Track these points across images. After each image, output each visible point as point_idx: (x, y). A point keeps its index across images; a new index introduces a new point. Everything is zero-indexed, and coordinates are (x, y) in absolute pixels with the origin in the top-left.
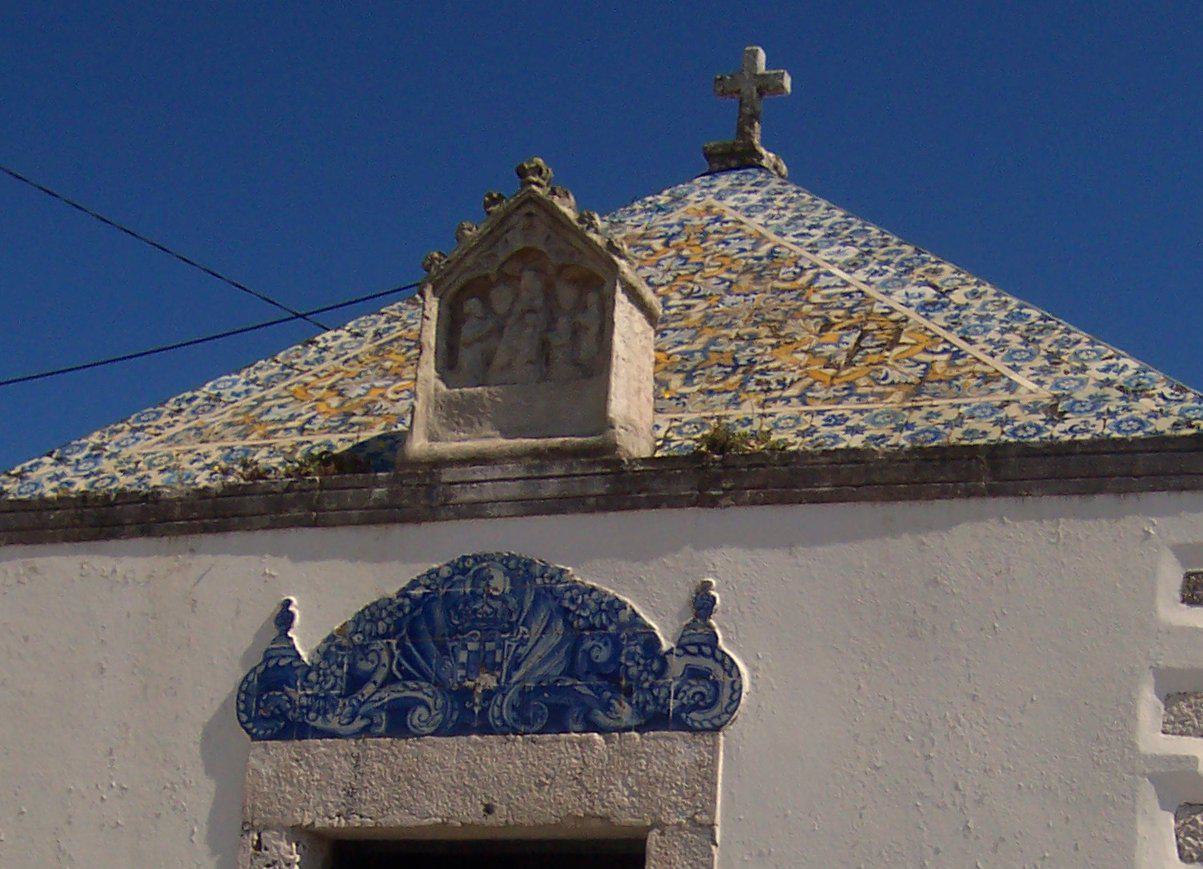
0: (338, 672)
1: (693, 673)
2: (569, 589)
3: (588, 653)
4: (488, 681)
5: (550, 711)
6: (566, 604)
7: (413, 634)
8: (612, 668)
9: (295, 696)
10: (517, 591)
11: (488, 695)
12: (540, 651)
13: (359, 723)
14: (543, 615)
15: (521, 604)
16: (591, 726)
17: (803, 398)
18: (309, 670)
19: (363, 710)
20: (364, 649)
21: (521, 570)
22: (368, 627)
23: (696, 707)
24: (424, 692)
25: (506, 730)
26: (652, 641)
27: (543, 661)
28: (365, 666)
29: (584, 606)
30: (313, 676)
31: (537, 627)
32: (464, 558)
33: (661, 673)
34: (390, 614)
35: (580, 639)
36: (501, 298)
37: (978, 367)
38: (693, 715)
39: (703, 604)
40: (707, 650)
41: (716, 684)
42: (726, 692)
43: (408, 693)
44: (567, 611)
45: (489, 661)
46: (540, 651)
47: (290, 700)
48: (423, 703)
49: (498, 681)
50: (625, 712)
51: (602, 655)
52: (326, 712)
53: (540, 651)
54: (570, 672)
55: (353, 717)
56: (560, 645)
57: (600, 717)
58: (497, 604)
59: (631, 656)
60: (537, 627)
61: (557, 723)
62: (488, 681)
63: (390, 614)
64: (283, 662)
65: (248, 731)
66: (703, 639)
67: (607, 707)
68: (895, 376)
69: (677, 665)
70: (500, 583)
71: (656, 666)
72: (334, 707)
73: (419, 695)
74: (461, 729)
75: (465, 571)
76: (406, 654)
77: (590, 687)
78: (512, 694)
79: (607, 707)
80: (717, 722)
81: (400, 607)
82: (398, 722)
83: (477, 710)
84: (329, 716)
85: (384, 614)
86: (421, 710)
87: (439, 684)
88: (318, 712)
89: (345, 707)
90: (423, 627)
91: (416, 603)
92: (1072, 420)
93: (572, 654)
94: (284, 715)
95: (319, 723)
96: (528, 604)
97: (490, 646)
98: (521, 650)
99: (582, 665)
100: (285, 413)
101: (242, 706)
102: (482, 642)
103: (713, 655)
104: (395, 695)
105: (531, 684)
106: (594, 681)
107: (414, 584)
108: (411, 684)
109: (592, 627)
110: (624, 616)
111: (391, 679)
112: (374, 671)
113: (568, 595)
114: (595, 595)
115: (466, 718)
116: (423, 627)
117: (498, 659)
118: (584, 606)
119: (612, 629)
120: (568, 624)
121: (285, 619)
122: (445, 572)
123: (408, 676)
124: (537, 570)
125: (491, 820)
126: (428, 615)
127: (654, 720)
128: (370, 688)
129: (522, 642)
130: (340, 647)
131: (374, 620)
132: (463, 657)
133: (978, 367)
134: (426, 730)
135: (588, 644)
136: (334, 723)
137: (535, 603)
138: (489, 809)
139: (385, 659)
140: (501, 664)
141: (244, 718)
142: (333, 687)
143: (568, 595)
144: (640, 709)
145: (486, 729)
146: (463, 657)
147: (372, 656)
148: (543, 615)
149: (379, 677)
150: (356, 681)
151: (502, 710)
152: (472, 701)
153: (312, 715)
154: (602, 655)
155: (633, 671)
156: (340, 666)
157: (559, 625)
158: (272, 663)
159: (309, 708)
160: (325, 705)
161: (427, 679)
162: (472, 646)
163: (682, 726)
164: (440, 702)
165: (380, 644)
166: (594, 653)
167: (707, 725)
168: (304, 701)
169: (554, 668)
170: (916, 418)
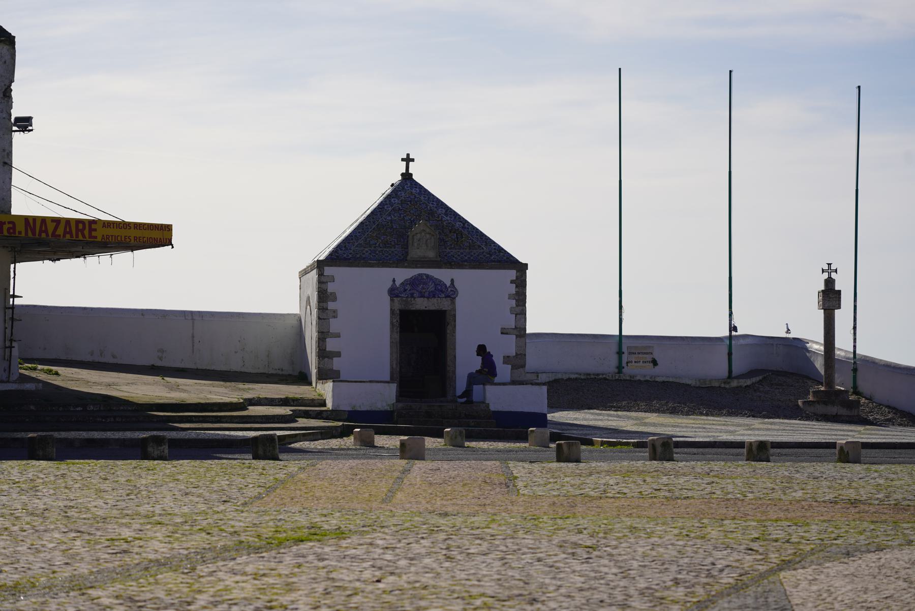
5: (433, 295)
12: (431, 287)
21: (427, 276)
39: (452, 280)
61: (434, 297)
82: (412, 296)
121: (394, 281)
127: (447, 296)
145: (424, 297)
150: (405, 290)
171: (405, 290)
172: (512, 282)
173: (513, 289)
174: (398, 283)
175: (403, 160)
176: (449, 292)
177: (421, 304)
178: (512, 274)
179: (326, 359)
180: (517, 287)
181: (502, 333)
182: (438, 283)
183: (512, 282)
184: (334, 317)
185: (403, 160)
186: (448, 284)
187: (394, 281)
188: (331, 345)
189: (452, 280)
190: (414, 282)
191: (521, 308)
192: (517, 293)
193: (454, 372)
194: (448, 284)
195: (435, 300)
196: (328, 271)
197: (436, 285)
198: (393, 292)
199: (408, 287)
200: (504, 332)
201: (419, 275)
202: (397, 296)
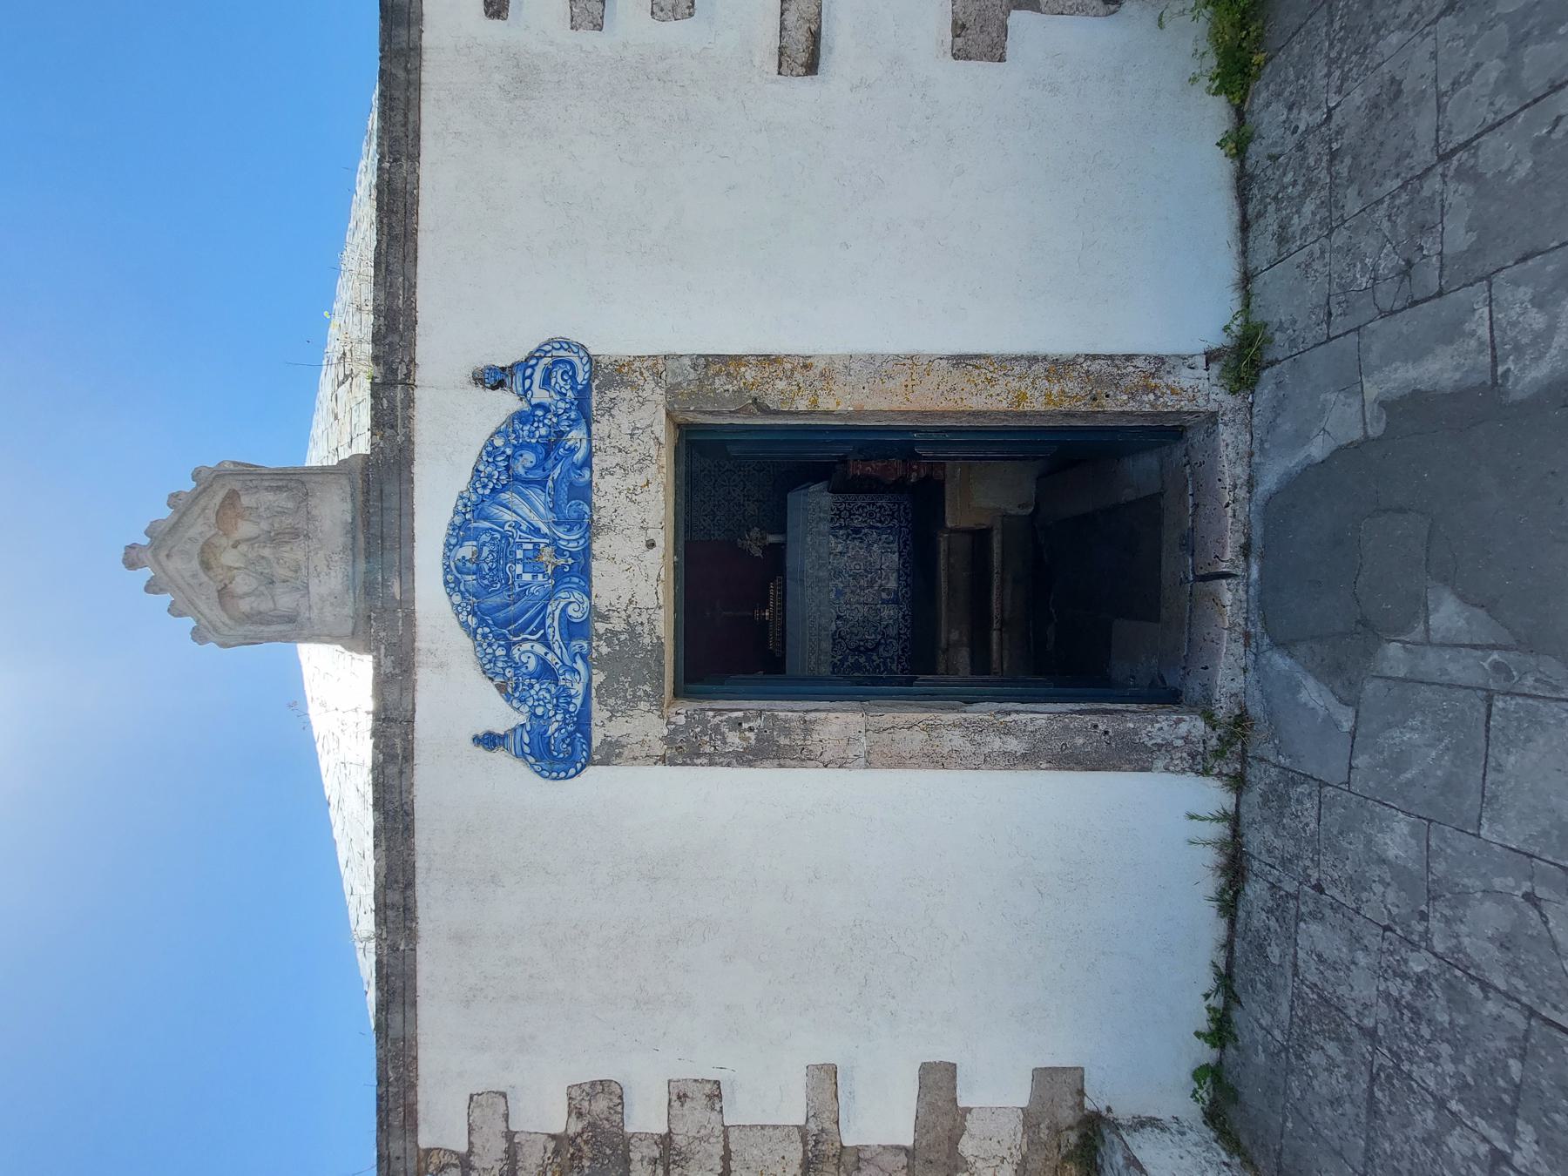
0: (537, 687)
2: (475, 490)
3: (528, 470)
6: (487, 492)
8: (540, 449)
9: (556, 725)
11: (559, 552)
13: (580, 665)
15: (486, 530)
16: (587, 463)
19: (568, 662)
21: (460, 532)
22: (500, 664)
24: (554, 608)
26: (521, 417)
28: (532, 664)
30: (539, 711)
31: (507, 516)
32: (446, 583)
34: (490, 645)
35: (517, 478)
38: (579, 379)
39: (494, 379)
40: (529, 372)
41: (555, 364)
42: (562, 353)
43: (556, 624)
44: (493, 490)
45: (530, 554)
47: (558, 730)
48: (564, 610)
49: (548, 545)
50: (576, 436)
51: (529, 458)
52: (570, 696)
54: (542, 484)
55: (575, 671)
56: (520, 494)
57: (579, 456)
58: (486, 550)
60: (507, 516)
61: (583, 493)
62: (547, 554)
63: (490, 645)
64: (526, 740)
65: (584, 767)
66: (519, 376)
67: (572, 451)
69: (539, 395)
70: (467, 550)
71: (540, 413)
72: (565, 689)
73: (557, 613)
74: (585, 573)
75: (457, 581)
76: (523, 629)
77: (554, 467)
78: (560, 532)
80: (585, 360)
81: (485, 636)
83: (571, 561)
84: (573, 692)
85: (489, 651)
88: (569, 703)
89: (565, 679)
93: (528, 483)
94: (570, 734)
95: (578, 701)
96: (487, 524)
97: (520, 554)
98: (524, 528)
99: (538, 474)
101: (563, 774)
102: (516, 561)
103: (532, 367)
104: (557, 636)
105: (551, 516)
106: (549, 464)
107: (464, 625)
108: (548, 622)
109: (508, 468)
111: (544, 641)
112: (537, 656)
113: (480, 491)
114: (481, 468)
115: (578, 570)
116: (501, 615)
117: (530, 546)
118: (490, 477)
119: (509, 451)
121: (489, 741)
122: (457, 599)
123: (542, 624)
125: (660, 542)
128: (550, 657)
130: (515, 689)
132: (527, 577)
134: (587, 603)
135: (521, 471)
136: (578, 688)
137: (486, 519)
139: (526, 646)
140: (535, 544)
141: (572, 771)
142: (549, 691)
143: (480, 491)
144: (573, 423)
145: (587, 551)
146: (527, 577)
147: (524, 659)
148: (495, 511)
149: (540, 649)
151: (570, 540)
152: (563, 566)
153: (572, 708)
155: (543, 431)
156: (531, 686)
157: (505, 496)
158: (527, 749)
159: (567, 711)
161: (545, 606)
162: (519, 568)
164: (563, 595)
165: (515, 652)
166: (529, 465)
167: (587, 368)
168: (559, 717)
169: (539, 498)
171: (546, 671)
179: (967, 1147)
184: (715, 1095)
187: (489, 741)
189: (494, 379)
194: (507, 403)
195: (608, 491)
197: (517, 481)
198: (559, 749)
199: (528, 652)
201: (452, 584)
202: (582, 722)
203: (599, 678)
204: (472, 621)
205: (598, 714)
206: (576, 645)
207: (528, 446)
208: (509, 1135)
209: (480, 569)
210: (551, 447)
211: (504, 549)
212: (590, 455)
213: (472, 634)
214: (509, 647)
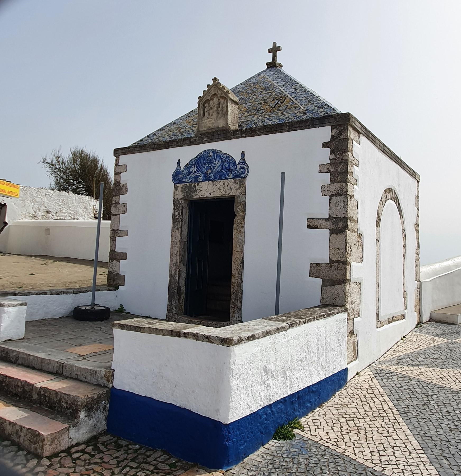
1: (241, 168)
4: (210, 171)
5: (219, 176)
7: (198, 164)
10: (214, 155)
11: (210, 174)
12: (218, 165)
13: (190, 180)
14: (218, 159)
16: (226, 178)
17: (264, 115)
18: (183, 171)
20: (191, 167)
21: (214, 151)
23: (242, 174)
24: (200, 174)
25: (213, 180)
26: (235, 162)
27: (218, 167)
28: (191, 170)
29: (224, 157)
31: (217, 162)
33: (236, 168)
35: (223, 163)
36: (211, 102)
37: (296, 105)
39: (243, 154)
46: (217, 166)
50: (231, 176)
51: (227, 165)
53: (217, 166)
54: (222, 169)
57: (227, 177)
59: (232, 165)
60: (217, 162)
62: (210, 171)
67: (228, 175)
68: (281, 109)
69: (239, 167)
70: (211, 154)
78: (214, 173)
79: (228, 175)
86: (200, 177)
87: (202, 173)
90: (199, 162)
91: (198, 159)
92: (307, 115)
99: (224, 168)
100: (184, 125)
107: (198, 155)
110: (230, 158)
111: (195, 172)
115: (207, 179)
116: (199, 162)
118: (224, 157)
120: (222, 160)
121: (179, 163)
122: (203, 153)
123: (198, 171)
124: (217, 151)
125: (211, 196)
126: (200, 160)
129: (215, 164)
131: (192, 162)
132: (206, 167)
133: (296, 105)
136: (186, 181)
138: (210, 194)
144: (233, 175)
146: (206, 167)
148: (218, 159)
149: (193, 172)
150: (190, 173)
151: (212, 176)
154: (227, 165)
160: (185, 177)
162: (207, 165)
163: (240, 177)
170: (281, 117)
171: (190, 173)
172: (325, 145)
173: (325, 156)
174: (182, 166)
175: (269, 51)
176: (235, 170)
177: (206, 190)
178: (325, 133)
180: (332, 152)
181: (309, 227)
182: (226, 159)
183: (325, 145)
184: (125, 212)
185: (269, 51)
186: (238, 159)
187: (179, 163)
188: (121, 244)
189: (243, 154)
190: (199, 162)
191: (339, 185)
192: (333, 162)
193: (240, 285)
194: (238, 159)
195: (220, 183)
196: (124, 159)
198: (177, 177)
199: (193, 169)
200: (312, 225)
201: (205, 152)
202: (181, 182)
203: (188, 184)
204: (198, 157)
205: (182, 185)
206: (194, 179)
207: (229, 165)
208: (120, 173)
209: (207, 157)
210: (230, 170)
211: (212, 162)
212: (227, 179)
213: (196, 157)
214: (194, 165)
